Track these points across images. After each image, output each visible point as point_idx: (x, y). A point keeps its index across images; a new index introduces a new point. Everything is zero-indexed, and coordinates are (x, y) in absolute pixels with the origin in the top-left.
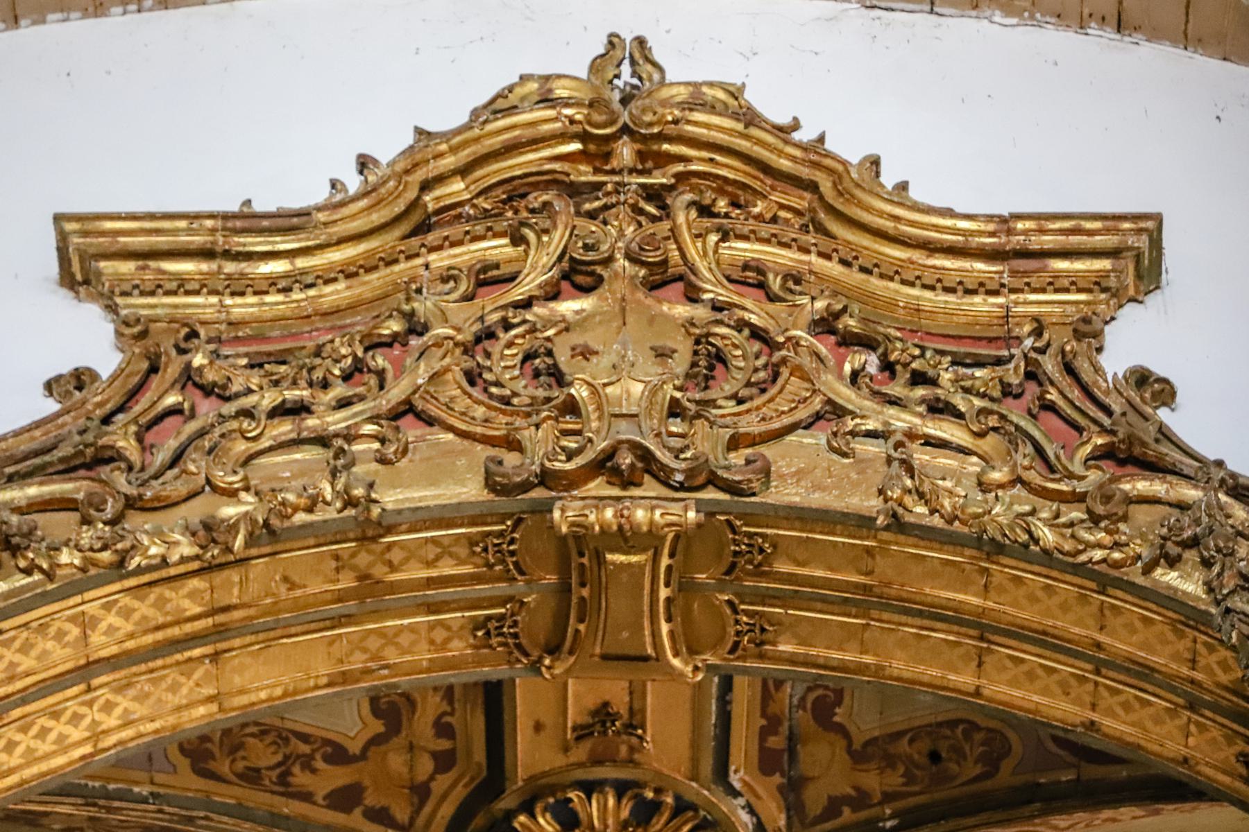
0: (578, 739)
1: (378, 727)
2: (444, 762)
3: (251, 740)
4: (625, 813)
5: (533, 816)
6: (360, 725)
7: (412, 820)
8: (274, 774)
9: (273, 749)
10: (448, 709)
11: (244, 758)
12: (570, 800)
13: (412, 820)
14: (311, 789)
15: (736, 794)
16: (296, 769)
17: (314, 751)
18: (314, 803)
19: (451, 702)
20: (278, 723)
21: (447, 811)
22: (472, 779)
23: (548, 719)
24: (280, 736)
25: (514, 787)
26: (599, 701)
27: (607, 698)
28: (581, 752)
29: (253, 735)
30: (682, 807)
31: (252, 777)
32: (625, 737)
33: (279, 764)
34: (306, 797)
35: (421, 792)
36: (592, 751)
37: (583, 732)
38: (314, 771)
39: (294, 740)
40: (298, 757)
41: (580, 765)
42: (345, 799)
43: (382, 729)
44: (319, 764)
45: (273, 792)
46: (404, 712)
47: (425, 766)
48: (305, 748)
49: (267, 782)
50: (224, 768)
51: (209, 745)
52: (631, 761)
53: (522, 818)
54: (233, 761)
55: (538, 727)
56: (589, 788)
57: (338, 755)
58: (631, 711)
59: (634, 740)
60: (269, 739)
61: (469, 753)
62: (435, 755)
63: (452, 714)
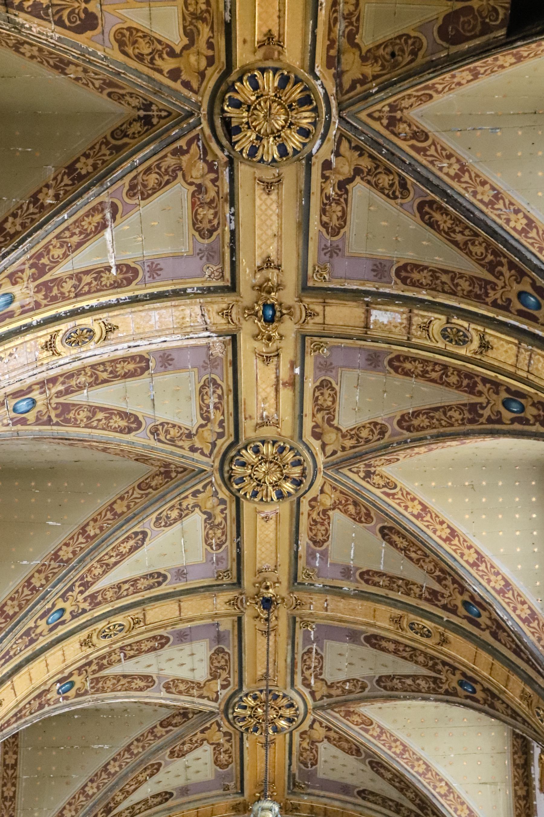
0: (259, 47)
1: (186, 41)
2: (211, 61)
3: (140, 40)
4: (276, 84)
5: (243, 84)
6: (180, 39)
7: (199, 88)
8: (149, 57)
9: (148, 45)
10: (212, 35)
11: (138, 48)
12: (256, 76)
13: (199, 88)
14: (162, 68)
15: (317, 78)
16: (157, 57)
17: (163, 49)
18: (163, 75)
19: (213, 32)
20: (149, 32)
21: (212, 84)
22: (221, 70)
23: (248, 38)
24: (150, 39)
25: (236, 70)
26: (267, 29)
27: (271, 27)
28: (260, 54)
29: (140, 37)
30: (297, 81)
31: (140, 58)
32: (276, 46)
33: (151, 54)
34: (160, 71)
35: (202, 75)
36: (265, 54)
37: (262, 45)
38: (163, 59)
39: (155, 42)
40: (158, 51)
41: (260, 60)
42: (175, 74)
43: (187, 42)
44: (165, 56)
45: (148, 67)
46: (195, 34)
47: (204, 63)
48: (160, 47)
49: (146, 62)
50: (130, 50)
51: (124, 38)
52: (279, 59)
53: (238, 84)
54: (134, 48)
55: (245, 41)
56: (263, 70)
57: (172, 54)
58: (279, 36)
59: (280, 48)
60: (147, 40)
61: (219, 59)
62: (207, 57)
63: (213, 38)
